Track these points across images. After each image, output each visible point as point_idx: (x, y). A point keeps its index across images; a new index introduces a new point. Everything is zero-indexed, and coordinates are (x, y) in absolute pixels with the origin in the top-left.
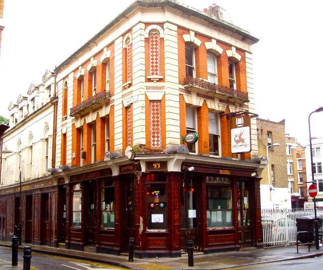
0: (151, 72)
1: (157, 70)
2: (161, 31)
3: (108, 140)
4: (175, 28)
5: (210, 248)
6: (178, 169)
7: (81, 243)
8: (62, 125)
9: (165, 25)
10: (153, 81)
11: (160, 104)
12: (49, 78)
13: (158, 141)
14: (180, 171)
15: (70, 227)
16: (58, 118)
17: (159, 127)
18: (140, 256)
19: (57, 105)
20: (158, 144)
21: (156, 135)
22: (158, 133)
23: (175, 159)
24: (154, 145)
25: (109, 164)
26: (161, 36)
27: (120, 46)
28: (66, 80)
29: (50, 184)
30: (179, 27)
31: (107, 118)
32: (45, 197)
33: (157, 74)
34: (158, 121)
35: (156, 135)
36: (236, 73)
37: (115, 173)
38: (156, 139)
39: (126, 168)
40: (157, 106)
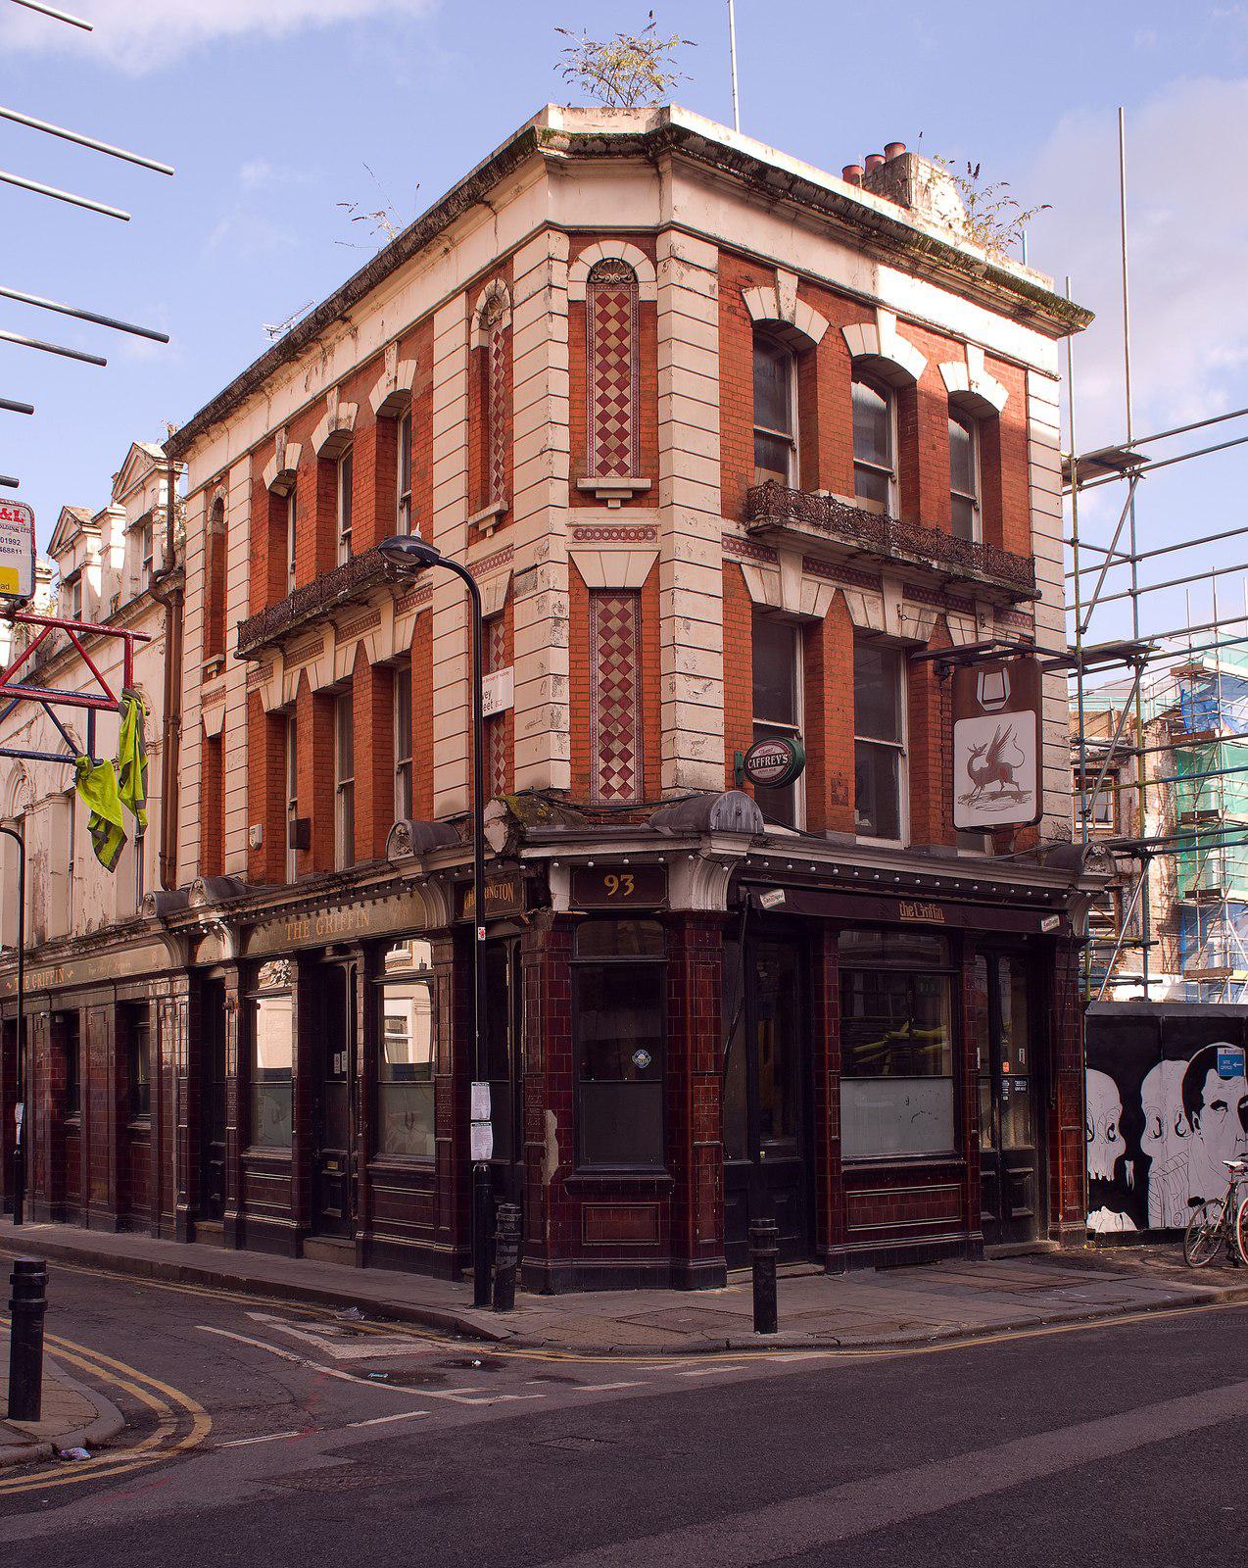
0: (599, 459)
1: (622, 451)
2: (644, 270)
4: (709, 256)
8: (205, 701)
10: (603, 502)
11: (638, 608)
13: (625, 773)
16: (186, 665)
17: (632, 712)
19: (181, 603)
20: (624, 788)
21: (616, 747)
22: (625, 737)
24: (607, 790)
26: (646, 293)
30: (727, 251)
33: (622, 469)
34: (625, 685)
35: (616, 747)
38: (616, 765)
40: (623, 616)
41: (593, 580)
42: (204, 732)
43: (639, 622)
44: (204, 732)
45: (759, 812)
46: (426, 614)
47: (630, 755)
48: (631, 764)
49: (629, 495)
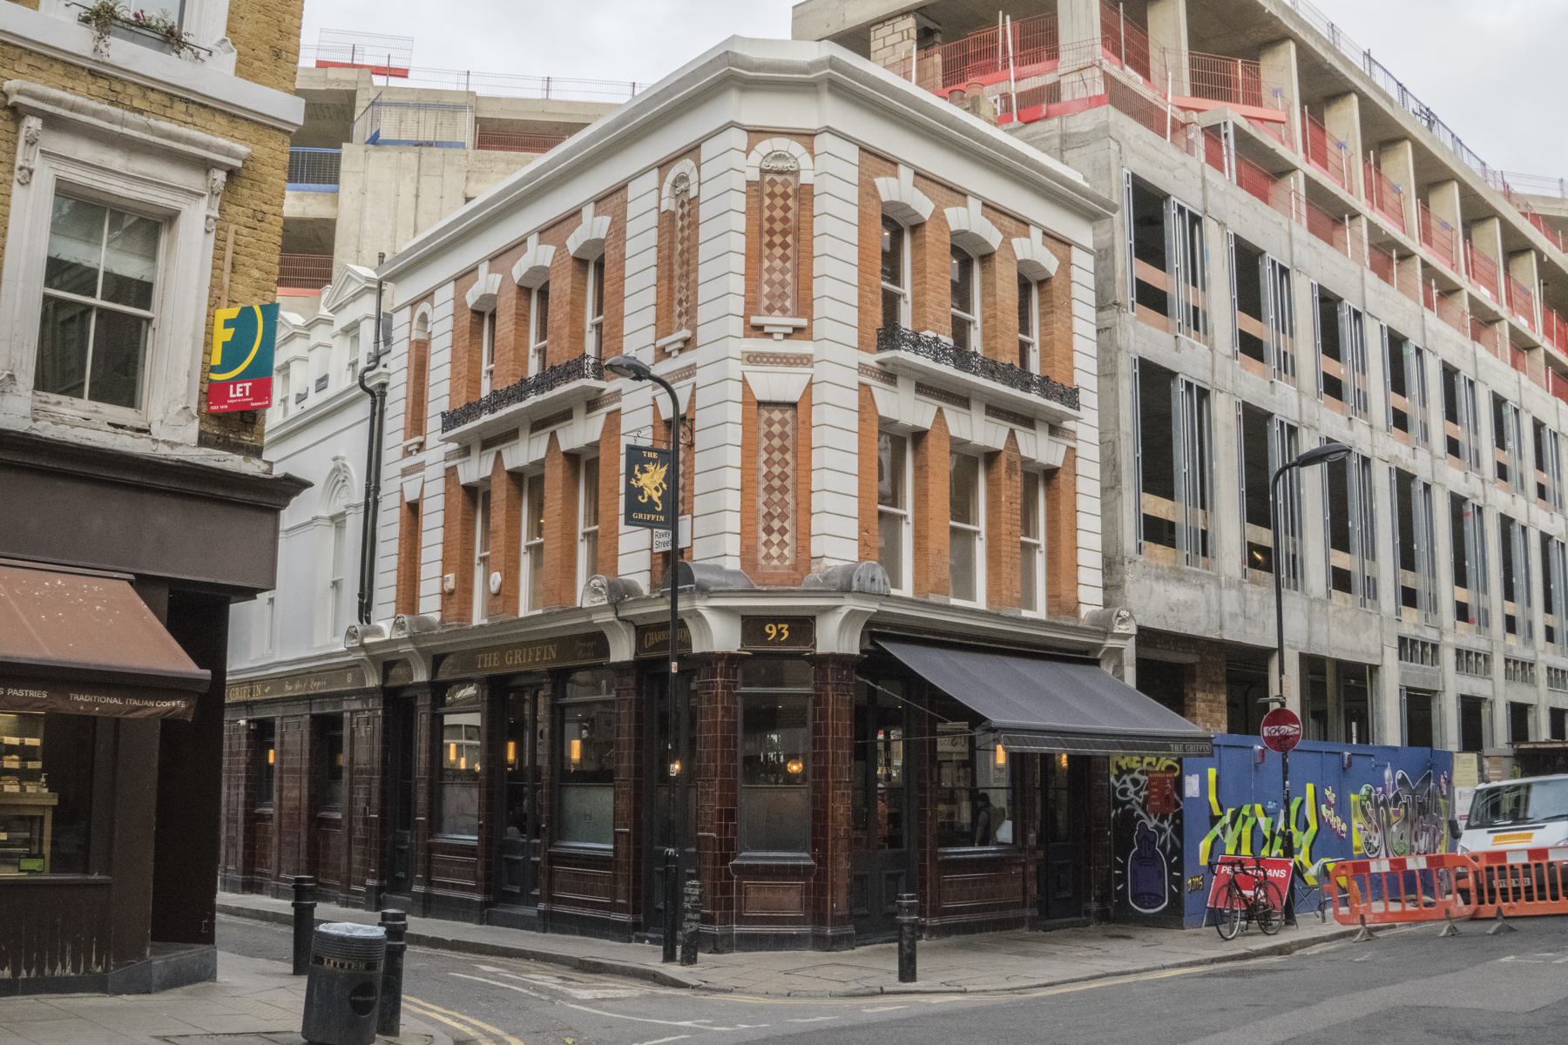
0: (766, 302)
1: (783, 296)
2: (805, 161)
3: (592, 537)
4: (853, 153)
5: (948, 920)
6: (850, 645)
7: (477, 898)
8: (405, 472)
9: (824, 143)
10: (770, 335)
11: (795, 417)
12: (356, 297)
13: (782, 544)
14: (857, 652)
15: (431, 836)
16: (388, 441)
17: (789, 497)
18: (720, 945)
19: (383, 395)
20: (781, 557)
21: (776, 524)
22: (783, 517)
23: (844, 611)
24: (768, 557)
25: (598, 619)
26: (805, 178)
27: (652, 200)
28: (424, 307)
29: (349, 683)
30: (864, 150)
31: (591, 456)
32: (326, 731)
33: (784, 311)
34: (783, 477)
35: (776, 524)
36: (1042, 315)
37: (622, 650)
38: (775, 538)
39: (660, 636)
40: (783, 423)
41: (761, 395)
42: (402, 496)
43: (795, 429)
44: (402, 496)
45: (887, 579)
46: (613, 416)
47: (786, 531)
48: (787, 538)
49: (790, 330)
